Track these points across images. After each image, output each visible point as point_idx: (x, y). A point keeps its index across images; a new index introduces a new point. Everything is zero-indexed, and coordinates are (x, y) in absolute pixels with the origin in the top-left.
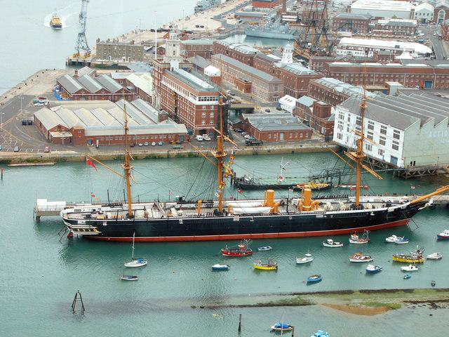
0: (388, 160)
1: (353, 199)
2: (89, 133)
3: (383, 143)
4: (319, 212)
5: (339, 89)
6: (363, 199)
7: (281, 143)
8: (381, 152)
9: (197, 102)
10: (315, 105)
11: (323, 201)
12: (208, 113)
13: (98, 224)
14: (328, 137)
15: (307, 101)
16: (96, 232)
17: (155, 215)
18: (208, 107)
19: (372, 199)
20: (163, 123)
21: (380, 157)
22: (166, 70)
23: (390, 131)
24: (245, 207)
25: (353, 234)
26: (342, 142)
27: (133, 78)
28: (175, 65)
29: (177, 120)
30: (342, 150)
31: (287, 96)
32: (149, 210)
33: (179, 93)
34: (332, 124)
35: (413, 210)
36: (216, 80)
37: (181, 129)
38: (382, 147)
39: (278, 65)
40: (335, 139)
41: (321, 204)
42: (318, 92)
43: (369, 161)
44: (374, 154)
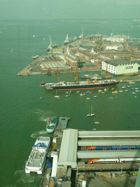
0: (113, 73)
1: (105, 81)
2: (51, 69)
3: (112, 69)
4: (98, 84)
5: (103, 58)
6: (108, 80)
7: (91, 70)
8: (112, 71)
9: (73, 62)
10: (98, 61)
11: (99, 81)
12: (76, 64)
13: (53, 87)
14: (101, 69)
15: (97, 60)
16: (52, 89)
17: (64, 85)
18: (76, 62)
19: (109, 80)
20: (66, 66)
21: (111, 72)
22: (67, 55)
23: (114, 67)
24: (82, 83)
25: (105, 88)
26: (104, 69)
27: (60, 56)
28: (69, 54)
29: (69, 66)
30: (103, 71)
31: (92, 60)
32: (63, 84)
33: (70, 60)
34: (101, 66)
35: (118, 83)
36: (77, 57)
37: (70, 67)
38: (112, 70)
39: (91, 53)
40: (102, 69)
41: (99, 82)
42: (99, 58)
43: (109, 73)
44: (110, 72)
